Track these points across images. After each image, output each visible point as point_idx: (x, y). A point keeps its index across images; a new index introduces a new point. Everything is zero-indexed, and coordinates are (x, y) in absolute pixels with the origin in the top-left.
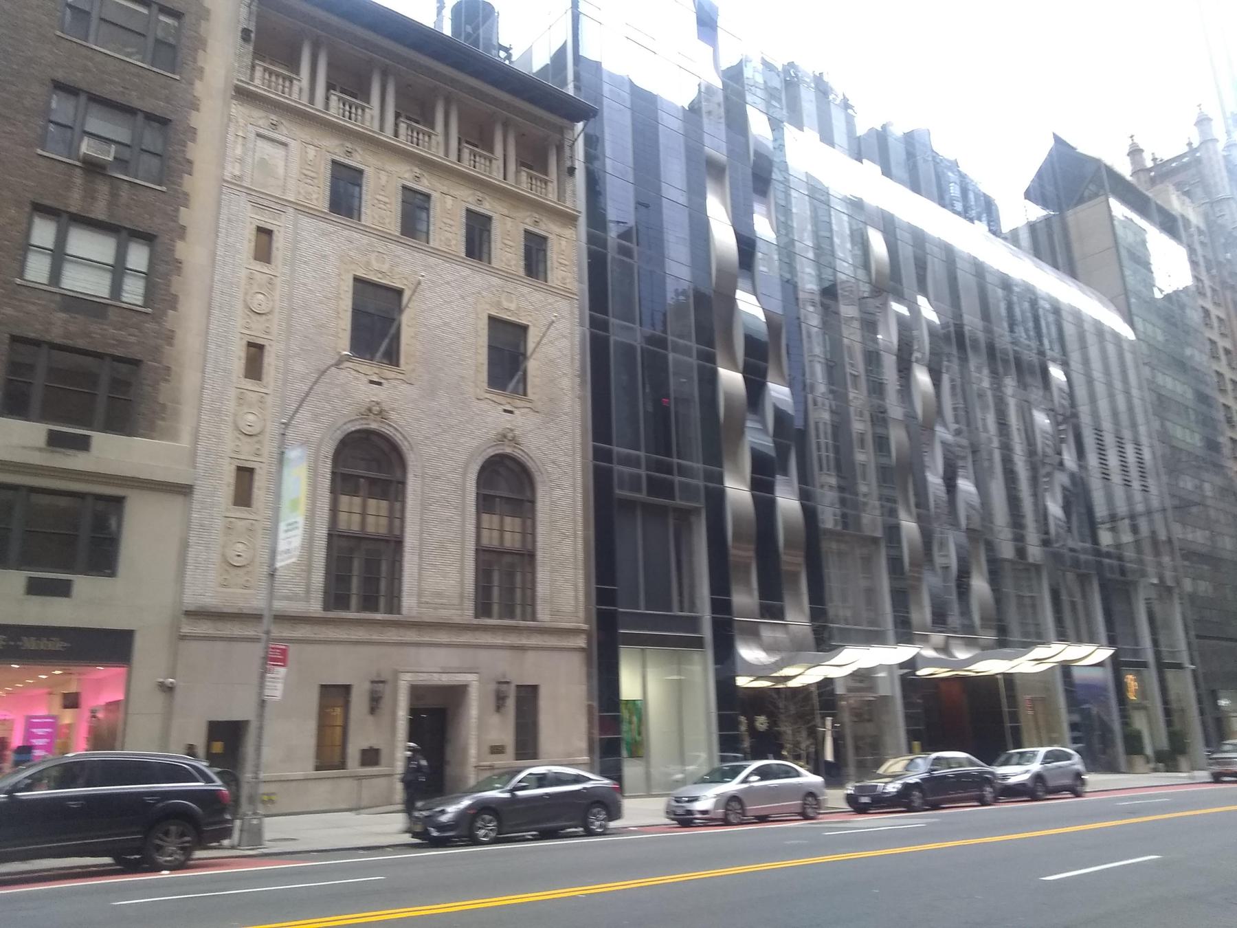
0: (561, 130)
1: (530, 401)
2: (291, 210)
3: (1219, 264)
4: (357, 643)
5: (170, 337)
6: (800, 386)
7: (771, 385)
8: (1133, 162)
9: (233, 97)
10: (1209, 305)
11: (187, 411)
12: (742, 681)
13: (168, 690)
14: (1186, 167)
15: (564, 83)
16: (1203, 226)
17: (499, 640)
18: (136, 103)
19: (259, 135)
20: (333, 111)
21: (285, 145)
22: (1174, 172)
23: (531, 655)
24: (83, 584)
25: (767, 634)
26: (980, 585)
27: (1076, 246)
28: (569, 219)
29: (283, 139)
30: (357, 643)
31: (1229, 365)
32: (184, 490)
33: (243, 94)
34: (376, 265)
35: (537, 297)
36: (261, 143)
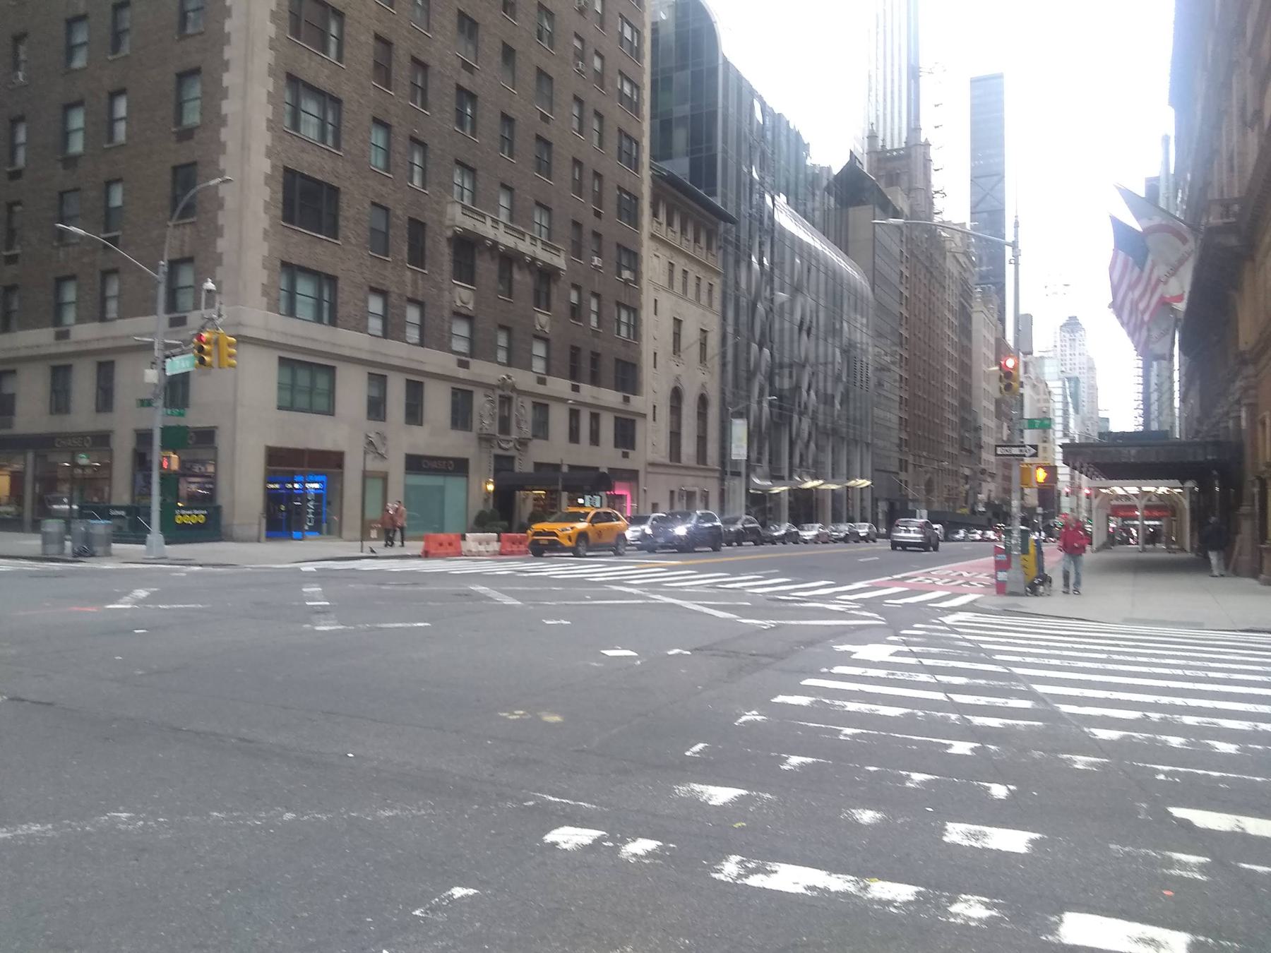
0: (717, 225)
5: (640, 353)
8: (870, 145)
10: (903, 269)
12: (751, 491)
13: (645, 491)
14: (899, 158)
15: (714, 194)
20: (669, 237)
22: (893, 159)
23: (708, 480)
24: (631, 453)
25: (758, 470)
26: (812, 445)
28: (718, 273)
32: (644, 416)
33: (653, 237)
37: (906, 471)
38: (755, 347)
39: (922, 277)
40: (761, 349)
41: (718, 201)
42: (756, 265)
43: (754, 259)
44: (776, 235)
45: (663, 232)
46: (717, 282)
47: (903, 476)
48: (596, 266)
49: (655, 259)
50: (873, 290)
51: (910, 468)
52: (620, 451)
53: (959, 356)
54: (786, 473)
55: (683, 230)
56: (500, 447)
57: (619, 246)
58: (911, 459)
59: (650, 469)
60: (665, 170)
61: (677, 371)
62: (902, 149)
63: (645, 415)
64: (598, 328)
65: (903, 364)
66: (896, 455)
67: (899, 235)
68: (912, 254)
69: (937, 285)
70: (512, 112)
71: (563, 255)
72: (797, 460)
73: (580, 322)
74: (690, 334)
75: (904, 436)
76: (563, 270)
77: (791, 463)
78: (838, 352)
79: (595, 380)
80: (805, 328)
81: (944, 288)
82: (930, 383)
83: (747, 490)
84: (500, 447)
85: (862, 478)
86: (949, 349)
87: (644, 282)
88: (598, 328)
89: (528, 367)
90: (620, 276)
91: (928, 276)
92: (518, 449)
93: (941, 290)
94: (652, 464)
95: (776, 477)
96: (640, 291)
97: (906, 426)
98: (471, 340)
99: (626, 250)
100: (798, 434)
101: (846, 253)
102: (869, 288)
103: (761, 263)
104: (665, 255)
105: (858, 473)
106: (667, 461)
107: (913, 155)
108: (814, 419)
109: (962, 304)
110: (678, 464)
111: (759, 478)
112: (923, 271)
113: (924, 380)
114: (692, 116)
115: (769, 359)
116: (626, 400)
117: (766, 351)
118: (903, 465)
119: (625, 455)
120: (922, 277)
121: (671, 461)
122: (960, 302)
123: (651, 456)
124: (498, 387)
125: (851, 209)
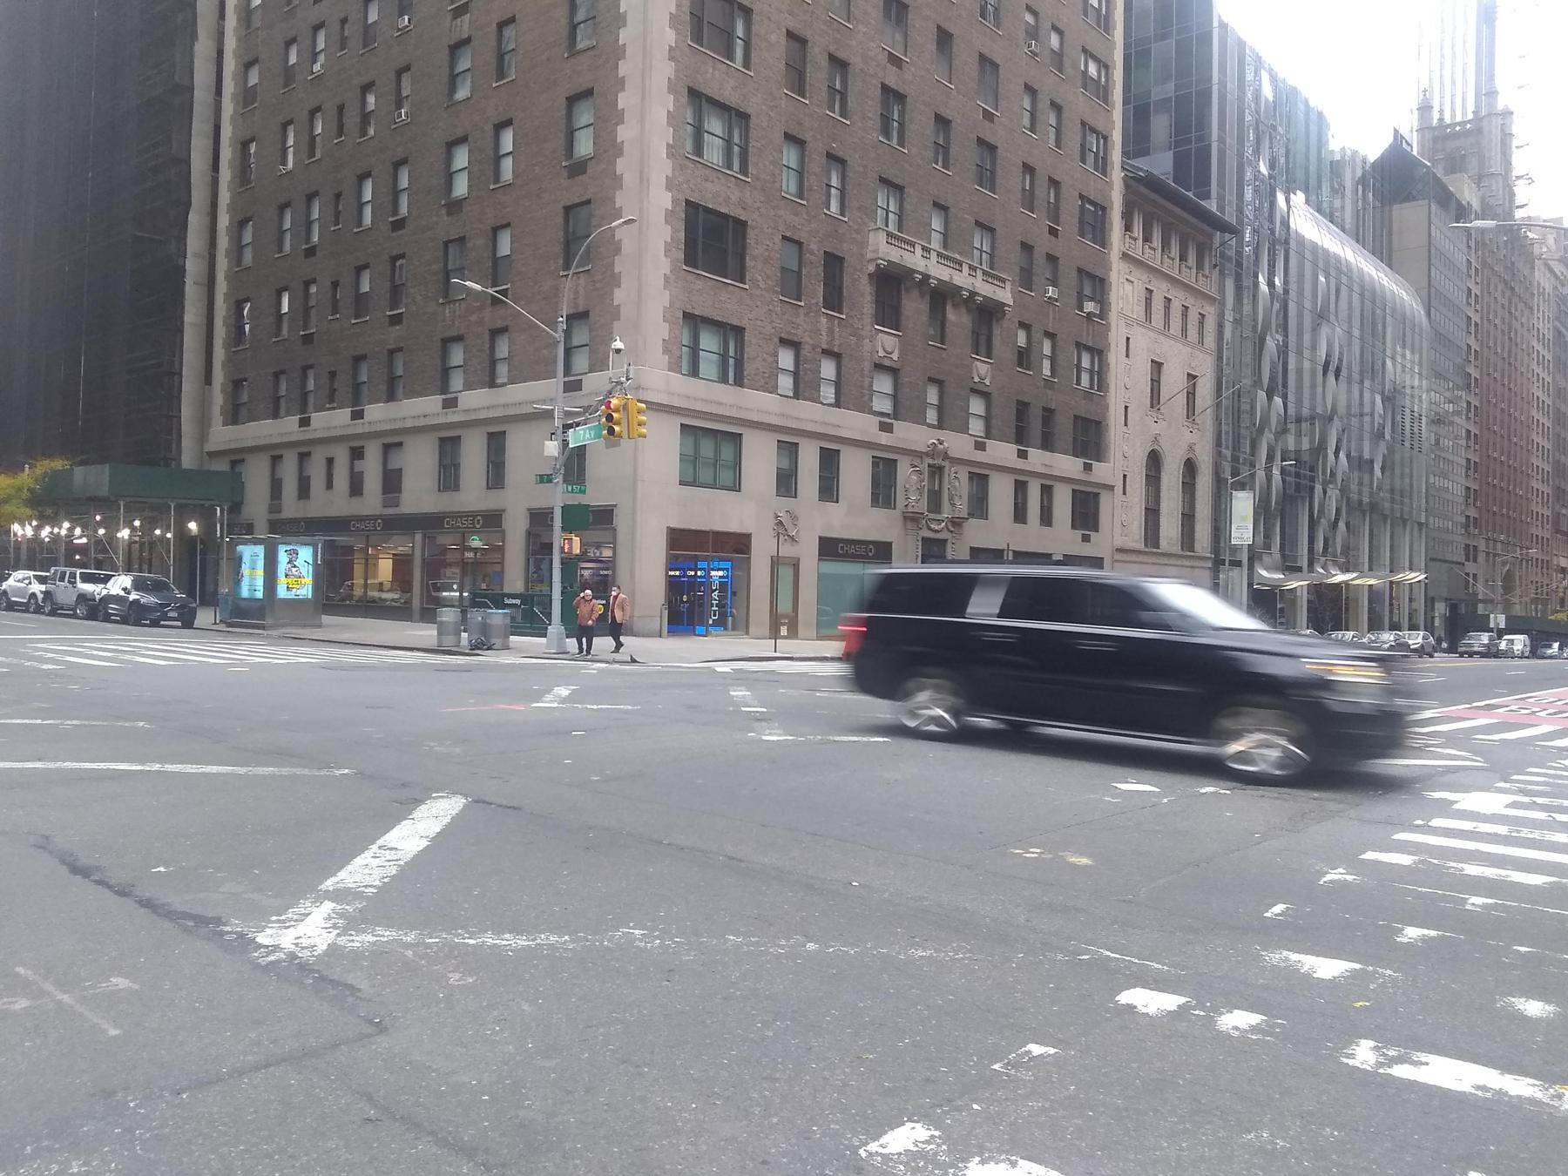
0: (1211, 237)
1: (1198, 424)
2: (1135, 324)
3: (1484, 244)
4: (1154, 564)
5: (1107, 407)
6: (1285, 397)
7: (1275, 397)
9: (1120, 258)
11: (1112, 448)
14: (1467, 133)
15: (1207, 196)
16: (1479, 211)
17: (1188, 563)
18: (1097, 274)
19: (1127, 279)
21: (1132, 282)
22: (1456, 136)
23: (1197, 570)
25: (1266, 559)
27: (1395, 238)
29: (1132, 279)
30: (1154, 564)
31: (1475, 337)
32: (1111, 488)
33: (1125, 256)
34: (1158, 351)
35: (1201, 356)
36: (1126, 283)
37: (1475, 560)
38: (1262, 395)
39: (1498, 295)
40: (1270, 398)
41: (1212, 206)
42: (1264, 287)
43: (1261, 279)
44: (1293, 244)
45: (1138, 249)
46: (1210, 311)
47: (1471, 567)
48: (1050, 298)
49: (1128, 287)
50: (1429, 315)
51: (1481, 558)
52: (1079, 533)
53: (1554, 403)
54: (1305, 563)
55: (1166, 245)
56: (930, 529)
57: (1080, 271)
58: (1482, 546)
59: (1118, 557)
60: (1141, 170)
61: (1156, 429)
62: (1469, 122)
63: (1113, 487)
64: (1051, 376)
65: (1472, 415)
66: (1459, 539)
67: (1465, 239)
68: (1484, 264)
69: (1521, 306)
70: (948, 111)
71: (1008, 286)
72: (1320, 545)
73: (1029, 370)
74: (1173, 381)
75: (1473, 513)
76: (1009, 306)
77: (1311, 550)
78: (1378, 399)
79: (1047, 444)
80: (1332, 368)
81: (1531, 309)
82: (1510, 440)
83: (1250, 585)
84: (930, 529)
85: (1411, 569)
86: (1539, 393)
87: (1113, 316)
88: (1051, 376)
89: (964, 429)
90: (1081, 308)
91: (1508, 293)
92: (952, 532)
93: (1527, 312)
94: (1120, 550)
95: (1291, 568)
96: (1107, 328)
97: (1475, 500)
98: (895, 398)
99: (1092, 277)
100: (1321, 511)
101: (1390, 266)
102: (1422, 312)
103: (1271, 284)
104: (1140, 280)
105: (1407, 564)
106: (1141, 546)
107: (1486, 129)
108: (1344, 490)
109: (1560, 332)
110: (1155, 550)
111: (1266, 569)
112: (1501, 287)
113: (1502, 437)
114: (1176, 97)
115: (1282, 411)
116: (1088, 467)
117: (1278, 401)
118: (1471, 553)
119: (1086, 539)
120: (1498, 295)
121: (1146, 545)
122: (1555, 328)
123: (1120, 541)
124: (927, 454)
125: (1395, 207)
